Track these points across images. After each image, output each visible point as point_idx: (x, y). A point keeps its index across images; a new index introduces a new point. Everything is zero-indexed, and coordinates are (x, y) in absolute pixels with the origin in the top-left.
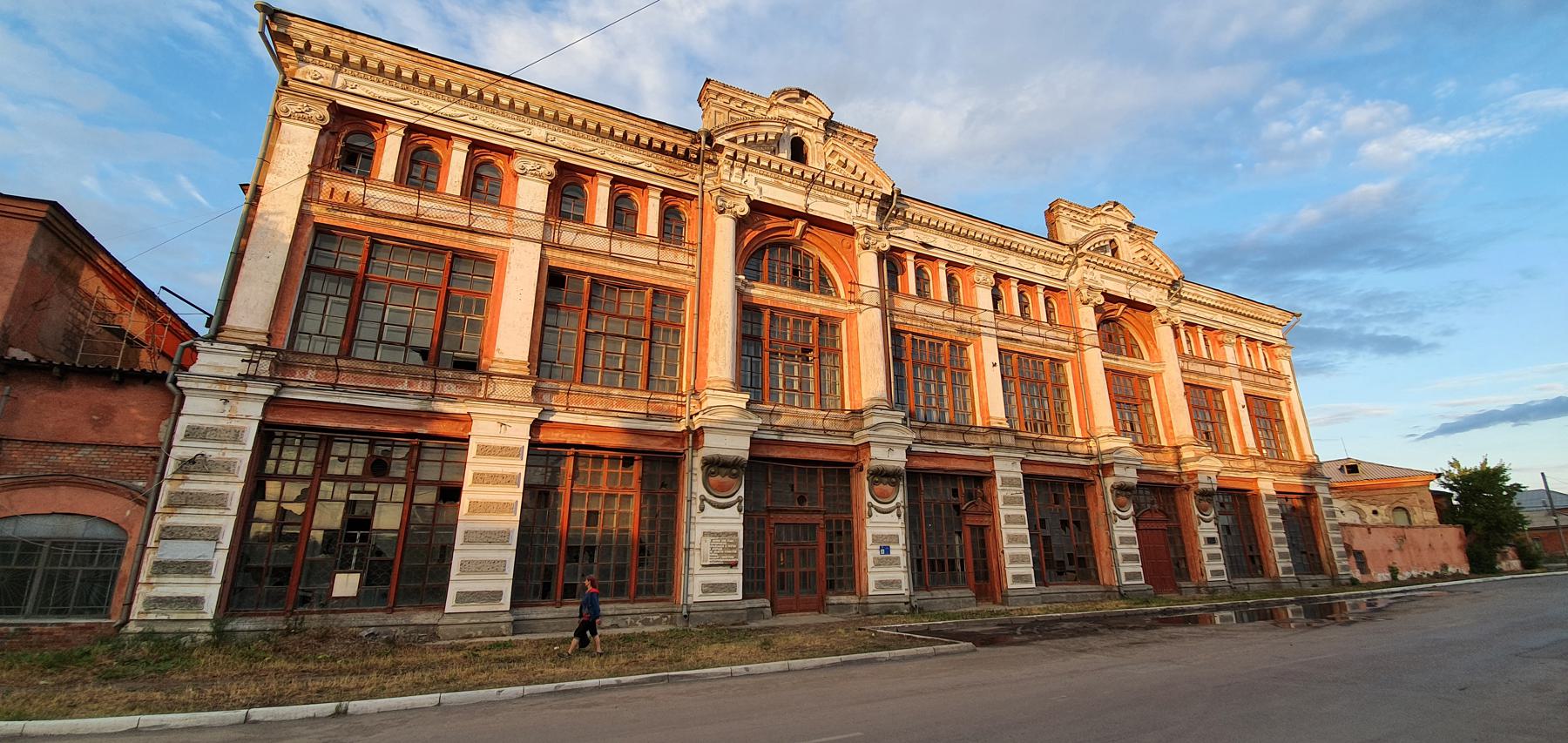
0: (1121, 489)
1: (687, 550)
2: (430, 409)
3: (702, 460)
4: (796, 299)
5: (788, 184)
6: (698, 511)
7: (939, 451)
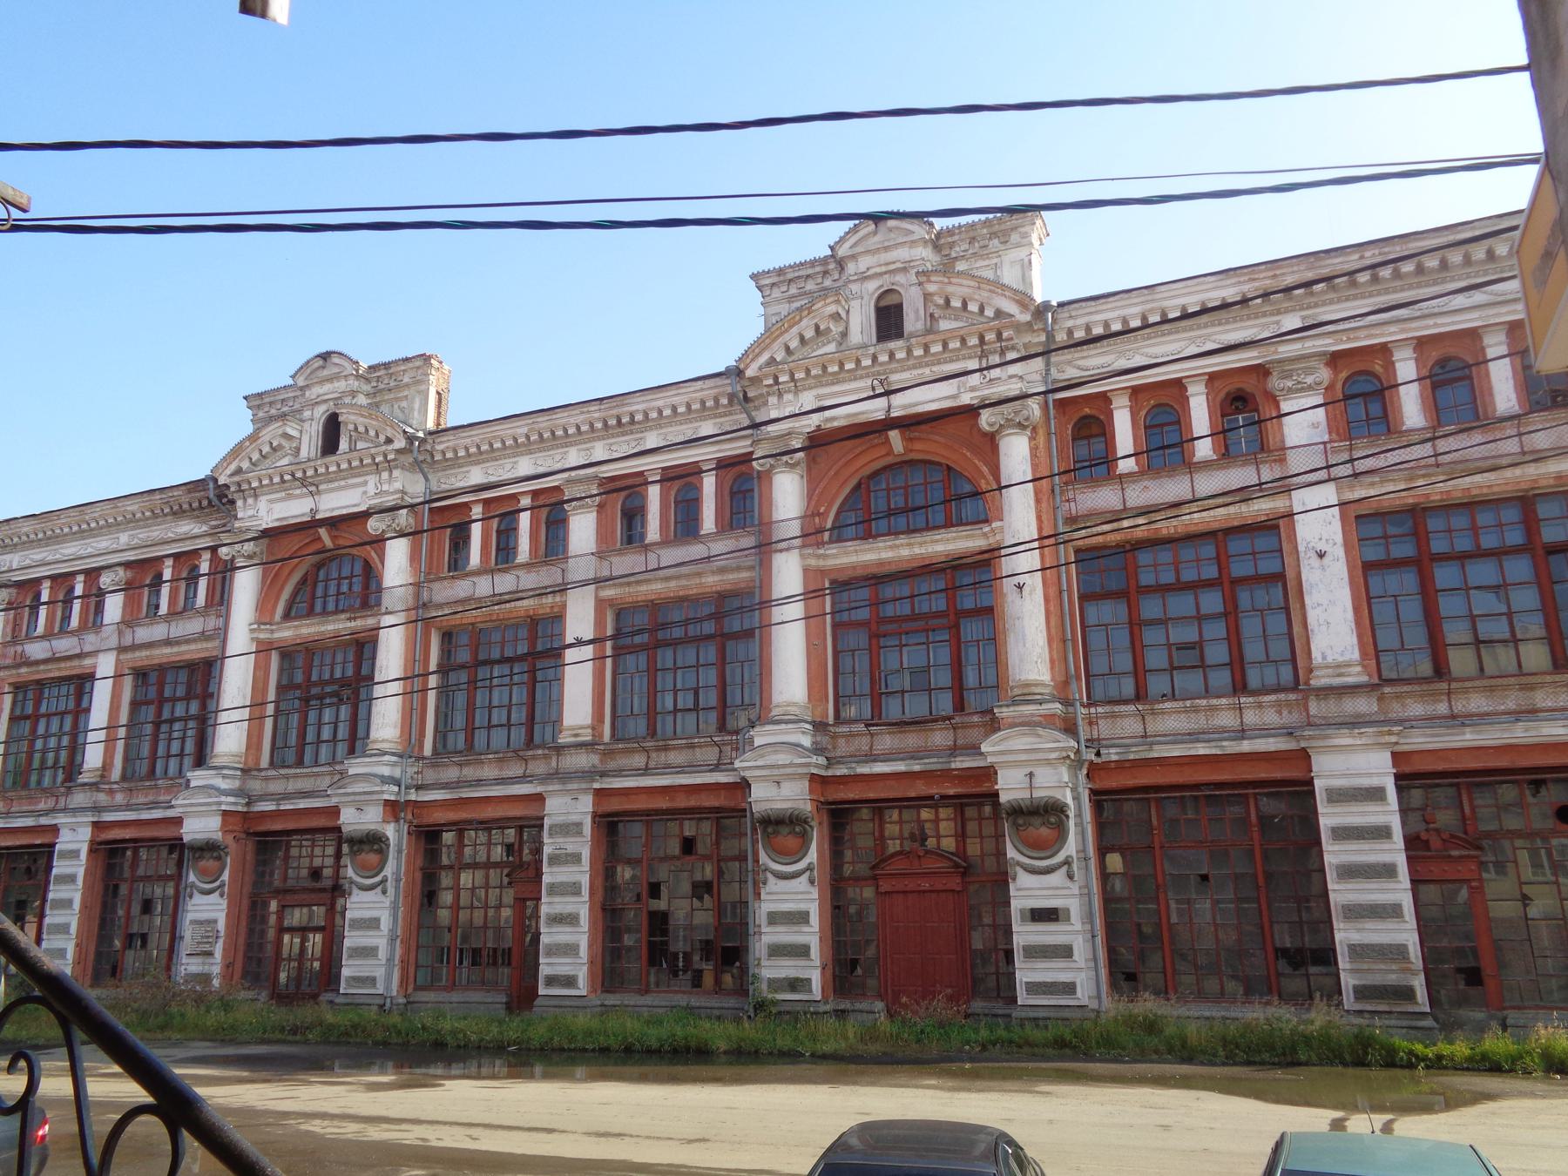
4: (323, 629)
5: (298, 492)
7: (464, 796)
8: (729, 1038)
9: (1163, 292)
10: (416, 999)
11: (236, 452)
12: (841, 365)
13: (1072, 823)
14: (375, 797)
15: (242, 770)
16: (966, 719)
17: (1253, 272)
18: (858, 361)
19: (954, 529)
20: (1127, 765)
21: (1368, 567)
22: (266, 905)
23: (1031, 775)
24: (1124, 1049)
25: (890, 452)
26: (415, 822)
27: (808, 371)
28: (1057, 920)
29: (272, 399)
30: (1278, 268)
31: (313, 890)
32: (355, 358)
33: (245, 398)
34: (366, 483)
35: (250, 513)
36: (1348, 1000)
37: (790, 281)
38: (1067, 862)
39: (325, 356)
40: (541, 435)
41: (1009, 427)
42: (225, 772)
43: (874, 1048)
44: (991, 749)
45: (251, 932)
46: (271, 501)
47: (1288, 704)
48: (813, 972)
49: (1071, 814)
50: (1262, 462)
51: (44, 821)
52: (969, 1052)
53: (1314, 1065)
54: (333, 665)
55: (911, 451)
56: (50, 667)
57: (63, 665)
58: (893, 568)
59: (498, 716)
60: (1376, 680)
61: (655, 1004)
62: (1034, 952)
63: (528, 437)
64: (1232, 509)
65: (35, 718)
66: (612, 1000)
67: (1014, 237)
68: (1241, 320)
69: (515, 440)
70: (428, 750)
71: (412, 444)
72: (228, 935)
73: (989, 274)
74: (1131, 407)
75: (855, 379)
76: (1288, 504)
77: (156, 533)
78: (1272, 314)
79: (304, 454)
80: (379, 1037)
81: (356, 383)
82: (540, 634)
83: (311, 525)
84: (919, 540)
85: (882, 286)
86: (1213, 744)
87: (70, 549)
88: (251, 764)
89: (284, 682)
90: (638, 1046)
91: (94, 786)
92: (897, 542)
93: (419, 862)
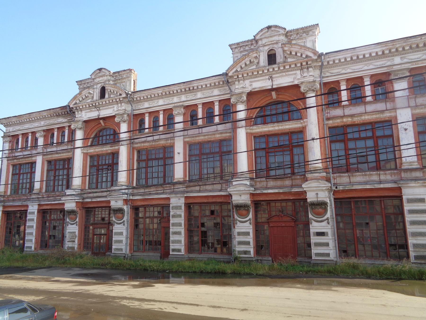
5: (94, 110)
8: (231, 269)
9: (357, 50)
10: (134, 255)
11: (75, 98)
12: (258, 72)
13: (329, 208)
14: (121, 198)
15: (81, 190)
16: (296, 177)
17: (387, 44)
18: (263, 71)
19: (292, 121)
20: (345, 191)
21: (420, 133)
22: (89, 228)
23: (317, 194)
24: (348, 274)
25: (272, 98)
26: (132, 205)
27: (248, 74)
28: (324, 235)
29: (84, 82)
30: (394, 42)
31: (102, 224)
32: (109, 70)
33: (76, 82)
34: (114, 107)
35: (80, 116)
36: (412, 259)
37: (241, 47)
38: (327, 219)
39: (100, 69)
40: (166, 93)
41: (310, 91)
42: (76, 190)
43: (274, 273)
44: (305, 186)
45: (85, 235)
46: (86, 112)
47: (394, 173)
48: (251, 249)
49: (329, 205)
50: (388, 102)
51: (24, 203)
52: (302, 274)
53: (407, 280)
54: (105, 160)
55: (278, 98)
56: (23, 160)
57: (27, 159)
58: (273, 133)
59: (155, 175)
60: (422, 167)
61: (204, 257)
62: (318, 245)
63: (162, 94)
64: (378, 116)
65: (19, 174)
66: (191, 256)
67: (311, 33)
68: (382, 58)
69: (158, 94)
70: (135, 185)
71: (127, 95)
72: (79, 236)
73: (303, 44)
74: (346, 85)
75: (262, 76)
76: (395, 114)
77: (52, 121)
78: (391, 56)
79: (95, 98)
80: (128, 267)
81: (110, 77)
82: (166, 151)
83: (99, 119)
84: (281, 124)
85: (269, 48)
86: (372, 185)
87: (27, 126)
88: (83, 188)
89: (91, 165)
90: (204, 271)
91: (38, 194)
92: (274, 125)
93: (133, 216)
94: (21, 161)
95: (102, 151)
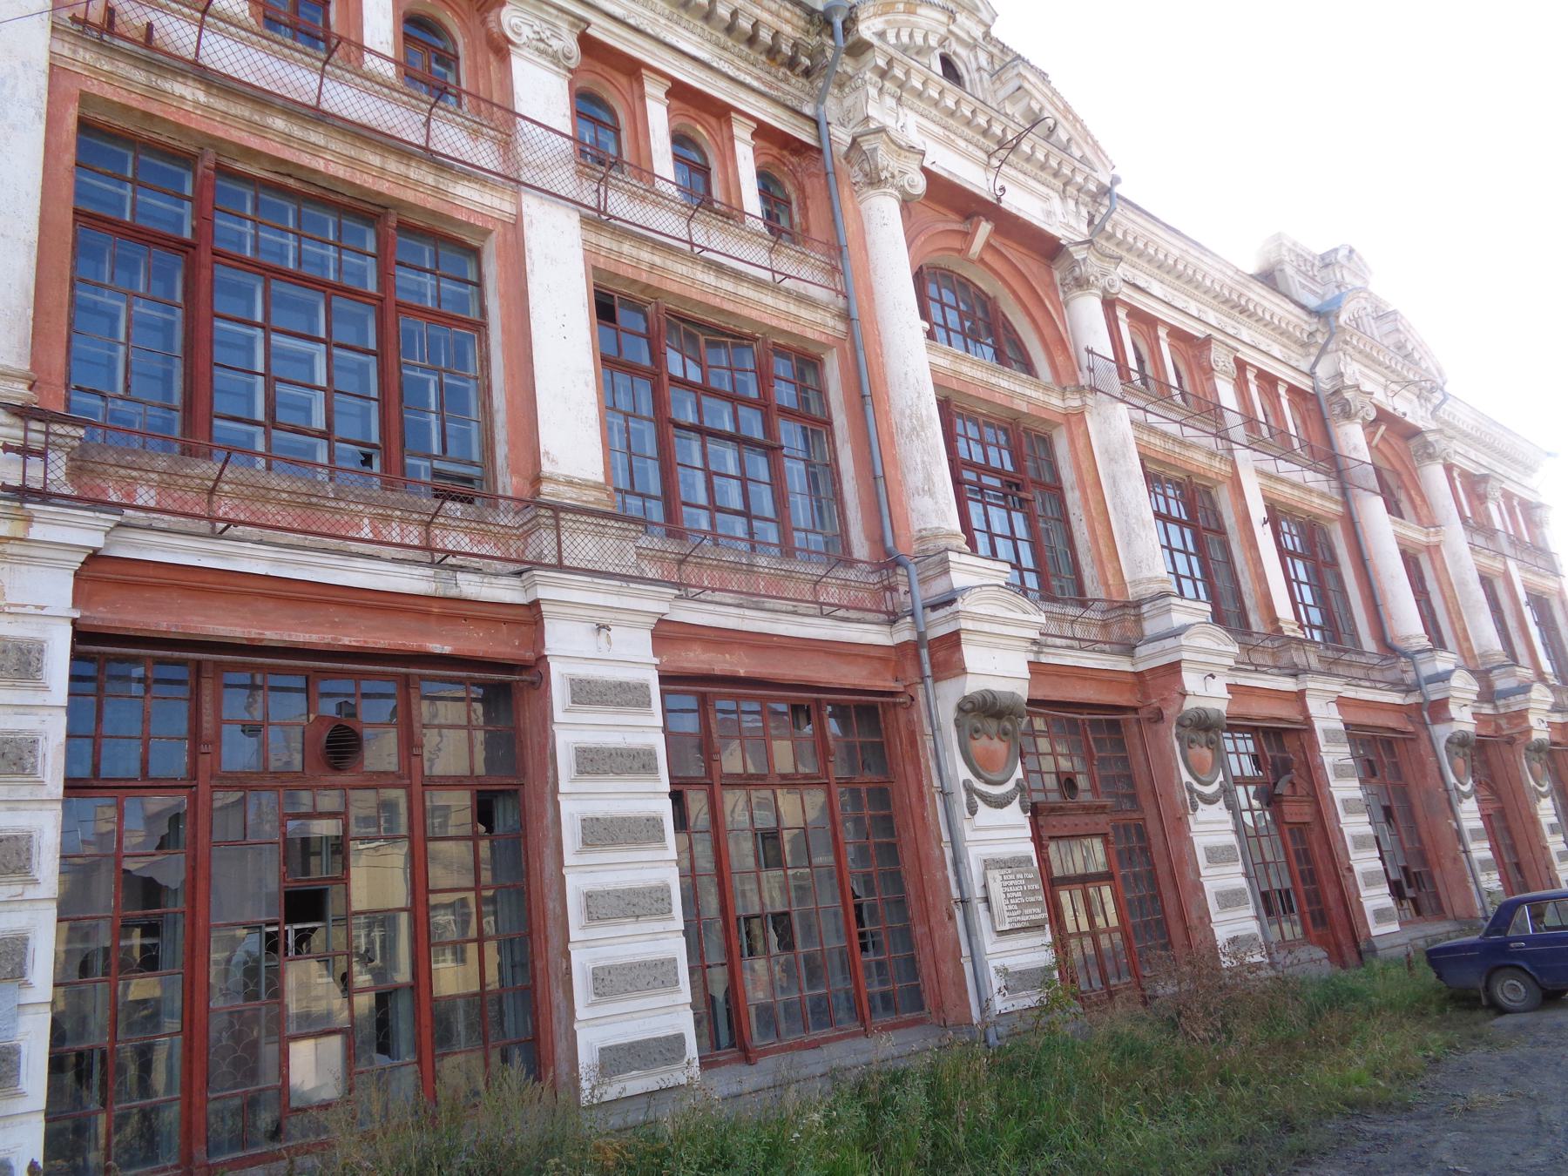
0: (1460, 743)
1: (964, 902)
2: (453, 592)
3: (960, 709)
4: (993, 380)
5: (962, 144)
6: (968, 816)
46: (920, 128)
56: (316, 137)
94: (288, 138)
95: (991, 387)
